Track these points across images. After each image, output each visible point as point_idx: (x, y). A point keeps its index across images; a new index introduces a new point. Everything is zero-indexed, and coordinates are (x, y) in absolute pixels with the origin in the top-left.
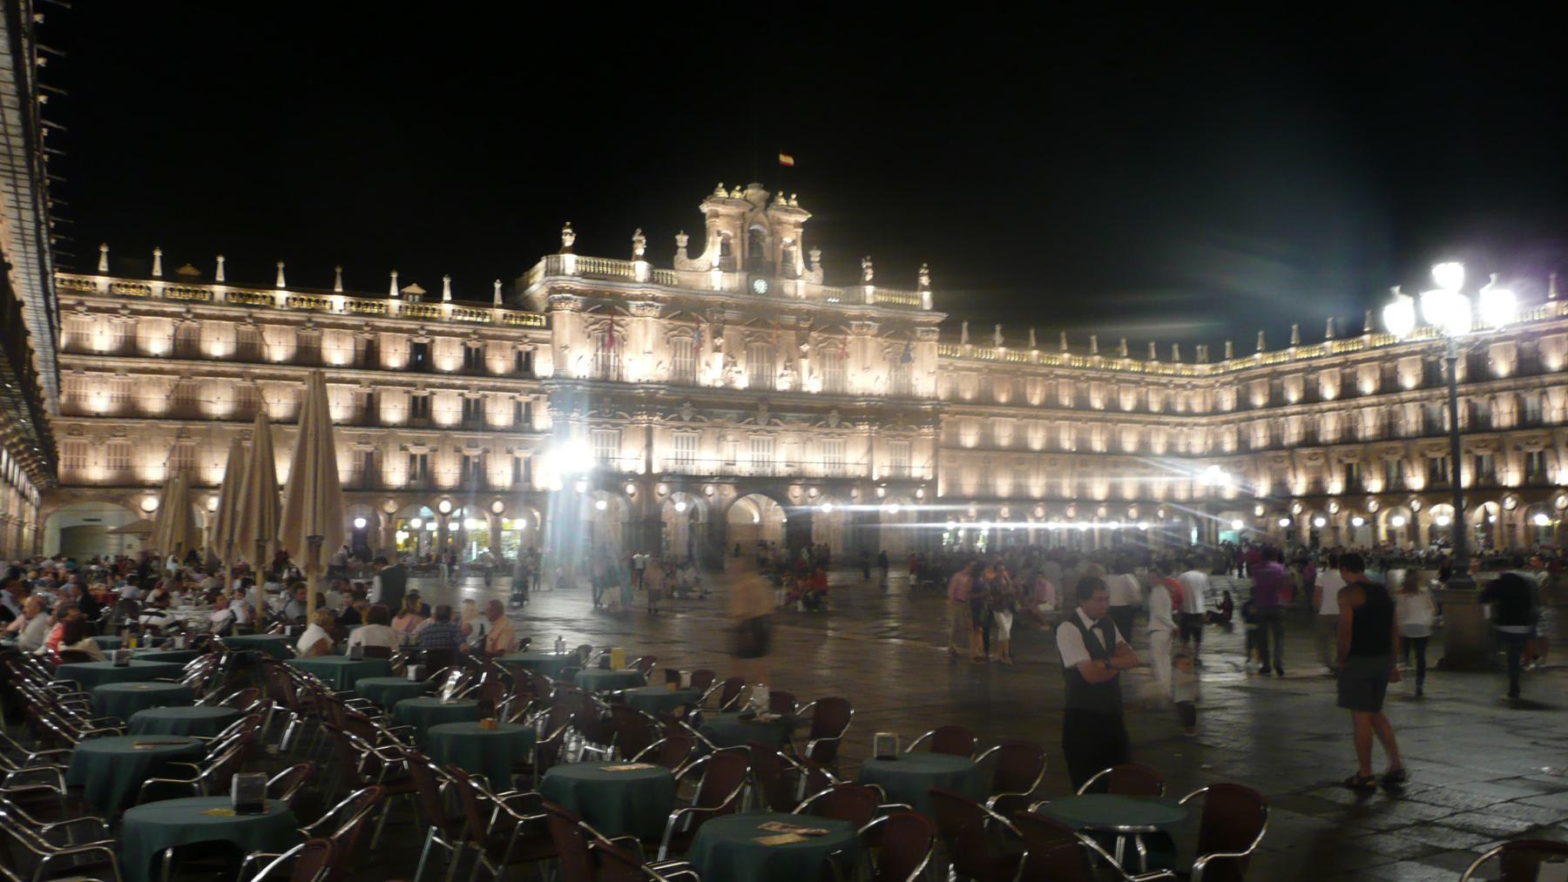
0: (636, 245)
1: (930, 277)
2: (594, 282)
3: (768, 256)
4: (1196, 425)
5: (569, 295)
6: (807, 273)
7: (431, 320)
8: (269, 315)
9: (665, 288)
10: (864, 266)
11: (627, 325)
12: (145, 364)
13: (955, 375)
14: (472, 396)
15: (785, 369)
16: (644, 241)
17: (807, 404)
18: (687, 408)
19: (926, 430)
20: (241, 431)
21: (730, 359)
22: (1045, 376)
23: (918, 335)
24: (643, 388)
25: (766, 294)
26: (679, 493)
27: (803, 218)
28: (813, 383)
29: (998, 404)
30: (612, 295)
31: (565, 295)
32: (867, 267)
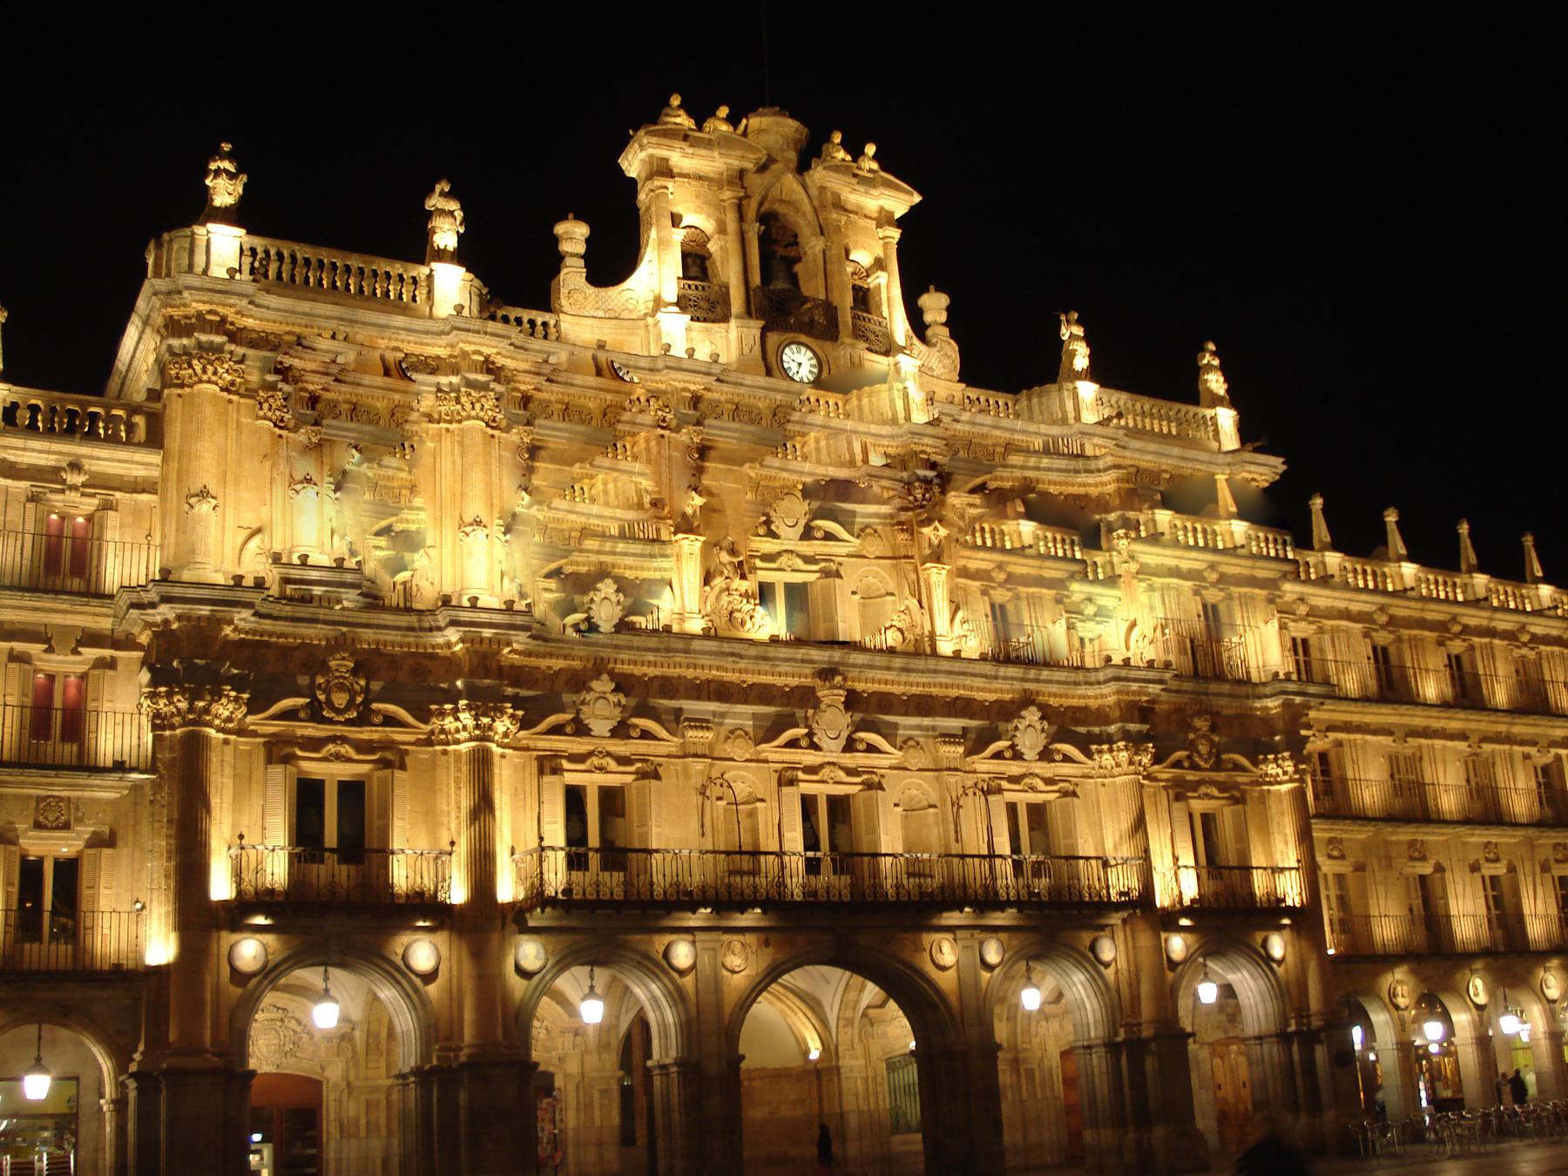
2: (305, 306)
3: (812, 287)
5: (219, 339)
10: (1065, 333)
16: (459, 214)
19: (1272, 769)
21: (725, 557)
22: (1510, 636)
24: (454, 623)
26: (581, 972)
27: (900, 201)
29: (1426, 705)
31: (204, 338)
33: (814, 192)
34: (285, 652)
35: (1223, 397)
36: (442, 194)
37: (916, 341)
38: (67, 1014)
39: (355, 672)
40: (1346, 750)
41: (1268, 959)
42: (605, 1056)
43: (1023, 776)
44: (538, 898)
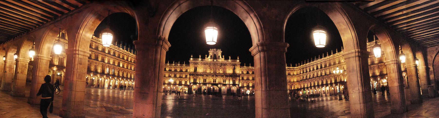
4: (295, 77)
6: (222, 59)
17: (220, 74)
25: (216, 61)
28: (221, 72)
30: (196, 62)
44: (201, 83)
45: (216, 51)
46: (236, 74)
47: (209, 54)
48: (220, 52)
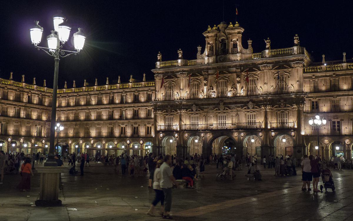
0: (180, 54)
1: (298, 40)
5: (157, 75)
6: (244, 51)
7: (127, 88)
8: (92, 93)
9: (186, 67)
11: (176, 81)
12: (70, 108)
13: (316, 80)
14: (136, 109)
15: (232, 88)
18: (194, 107)
20: (86, 123)
23: (292, 66)
30: (172, 72)
32: (267, 42)
33: (227, 33)
34: (165, 106)
35: (296, 44)
36: (179, 50)
37: (244, 49)
38: (150, 141)
39: (170, 107)
40: (321, 101)
41: (291, 136)
42: (217, 145)
43: (250, 111)
45: (226, 28)
46: (288, 93)
47: (206, 42)
48: (236, 31)
